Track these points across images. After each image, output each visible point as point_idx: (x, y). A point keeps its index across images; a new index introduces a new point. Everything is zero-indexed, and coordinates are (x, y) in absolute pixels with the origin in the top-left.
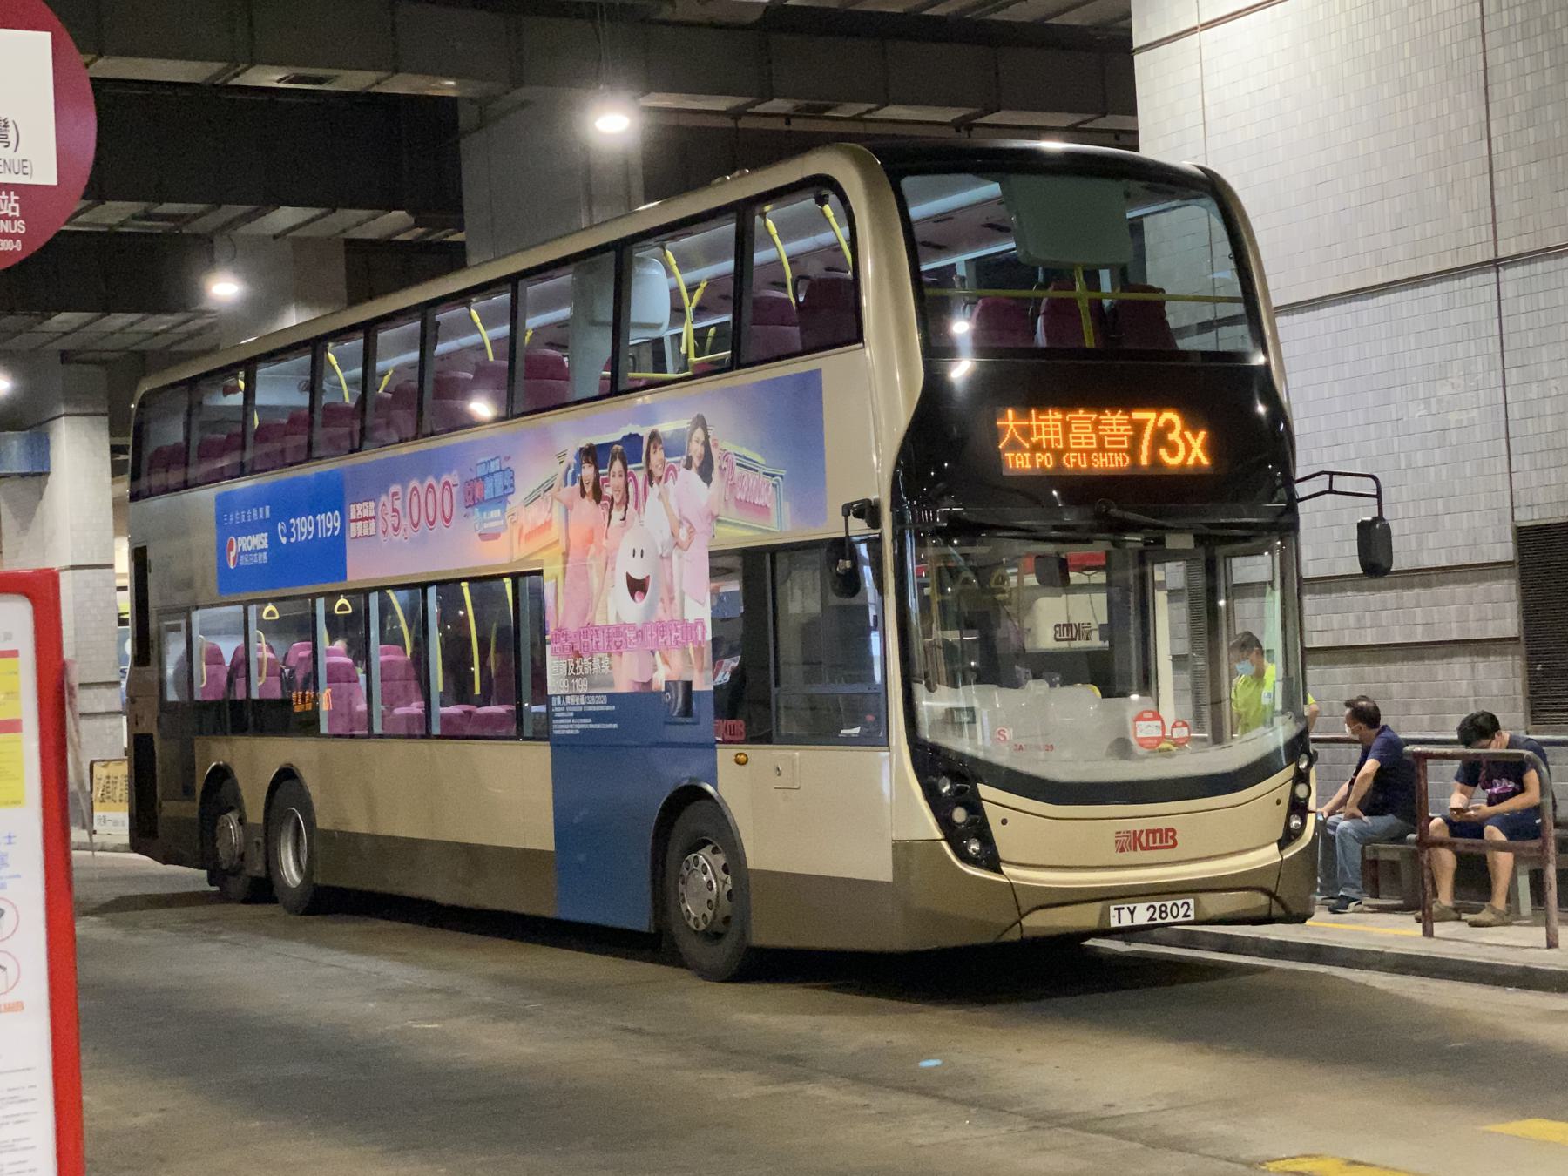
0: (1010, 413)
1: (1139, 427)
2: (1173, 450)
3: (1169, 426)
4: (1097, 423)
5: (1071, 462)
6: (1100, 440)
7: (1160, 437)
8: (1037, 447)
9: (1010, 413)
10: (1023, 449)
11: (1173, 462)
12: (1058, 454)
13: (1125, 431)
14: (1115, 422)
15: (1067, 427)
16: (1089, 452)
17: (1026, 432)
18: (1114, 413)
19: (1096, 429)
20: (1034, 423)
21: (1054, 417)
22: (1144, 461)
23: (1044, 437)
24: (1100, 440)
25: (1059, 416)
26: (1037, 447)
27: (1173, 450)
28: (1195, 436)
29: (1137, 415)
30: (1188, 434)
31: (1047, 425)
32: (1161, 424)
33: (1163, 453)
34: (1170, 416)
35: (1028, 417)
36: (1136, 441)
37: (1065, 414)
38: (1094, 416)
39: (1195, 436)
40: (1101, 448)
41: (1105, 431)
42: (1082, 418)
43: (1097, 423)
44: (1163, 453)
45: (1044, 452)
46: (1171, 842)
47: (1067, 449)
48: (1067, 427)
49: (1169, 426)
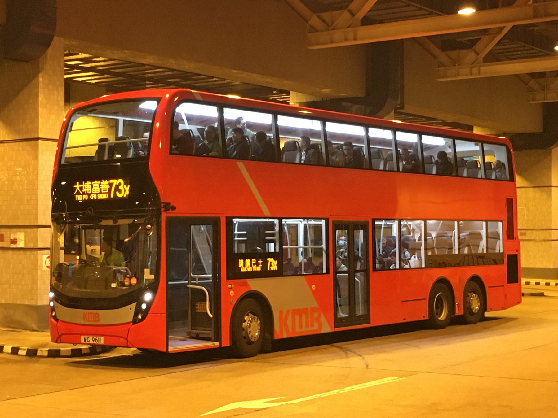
0: (78, 183)
1: (111, 185)
2: (120, 191)
3: (120, 184)
4: (100, 185)
5: (92, 197)
6: (100, 189)
7: (117, 189)
8: (84, 193)
9: (78, 183)
10: (78, 193)
11: (119, 195)
12: (89, 195)
13: (107, 187)
14: (105, 184)
15: (92, 186)
16: (97, 194)
17: (81, 189)
18: (105, 180)
19: (100, 187)
20: (83, 186)
21: (89, 183)
22: (112, 196)
23: (86, 190)
24: (100, 189)
25: (90, 183)
26: (84, 193)
27: (120, 191)
28: (127, 186)
29: (111, 181)
30: (125, 186)
31: (87, 186)
32: (118, 184)
33: (117, 193)
34: (121, 181)
35: (82, 184)
36: (110, 189)
37: (91, 182)
38: (99, 182)
39: (127, 186)
40: (101, 193)
41: (102, 187)
42: (96, 183)
43: (100, 185)
44: (117, 193)
45: (85, 194)
46: (97, 319)
47: (92, 193)
48: (92, 186)
49: (120, 184)
